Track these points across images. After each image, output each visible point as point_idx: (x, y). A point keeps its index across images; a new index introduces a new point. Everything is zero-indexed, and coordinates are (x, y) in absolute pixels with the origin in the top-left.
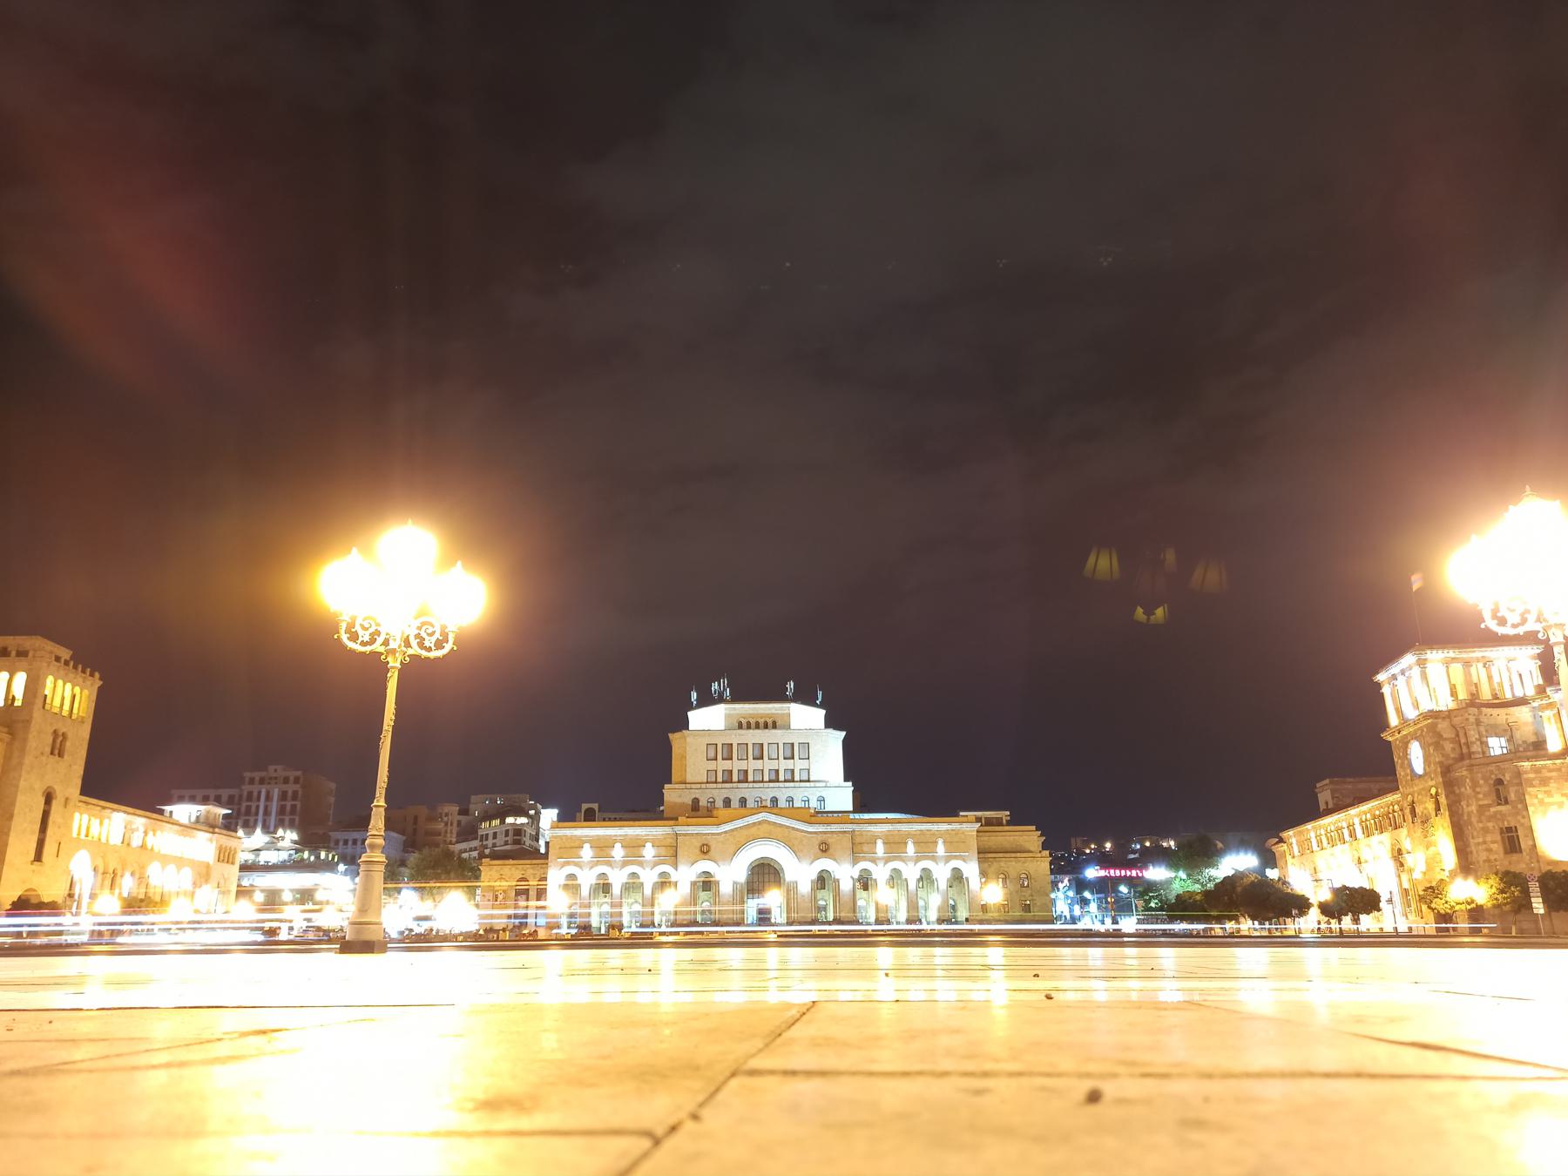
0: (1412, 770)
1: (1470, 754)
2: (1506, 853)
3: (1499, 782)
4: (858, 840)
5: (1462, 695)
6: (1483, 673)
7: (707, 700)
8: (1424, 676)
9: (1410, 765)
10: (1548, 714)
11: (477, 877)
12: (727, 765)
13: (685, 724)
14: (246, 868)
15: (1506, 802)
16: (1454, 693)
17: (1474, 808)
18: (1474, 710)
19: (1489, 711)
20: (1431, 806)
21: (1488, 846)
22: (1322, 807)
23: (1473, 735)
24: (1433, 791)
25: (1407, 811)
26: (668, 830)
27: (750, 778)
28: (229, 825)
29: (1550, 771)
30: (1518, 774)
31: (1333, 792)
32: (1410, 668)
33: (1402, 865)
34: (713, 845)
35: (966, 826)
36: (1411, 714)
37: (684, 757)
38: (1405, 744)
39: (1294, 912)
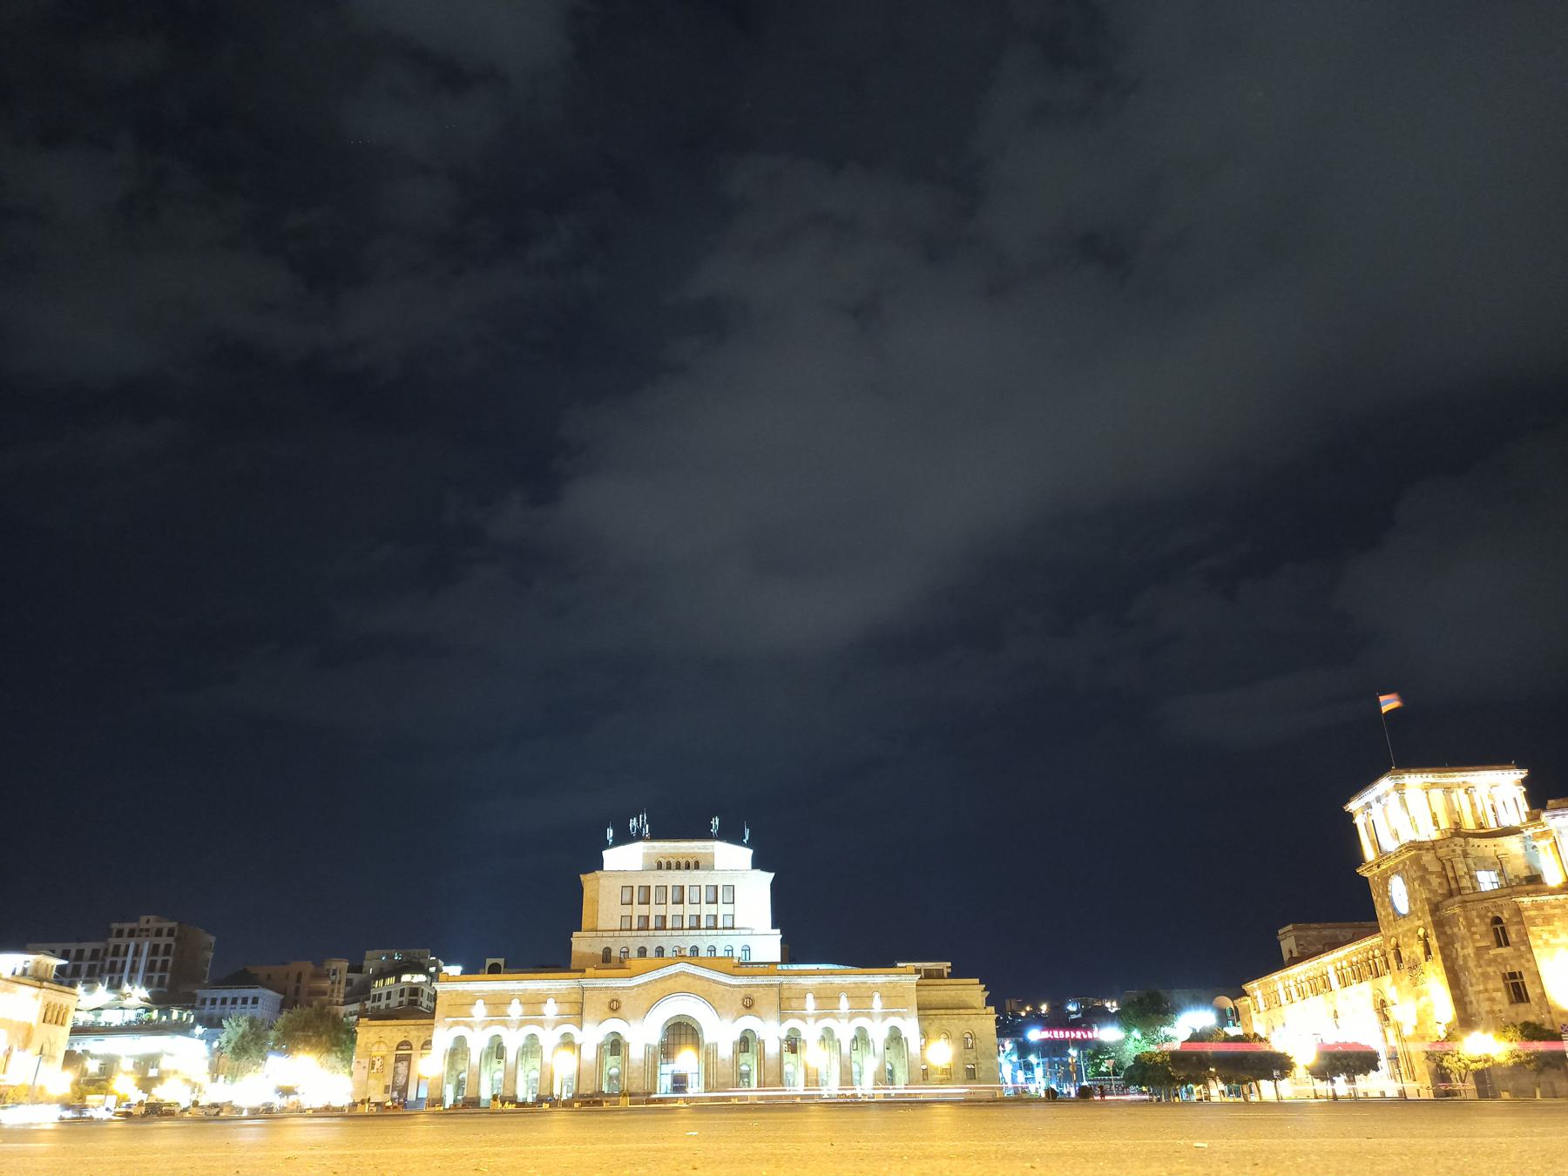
0: (1395, 909)
1: (1459, 889)
2: (1512, 1003)
3: (1497, 920)
4: (786, 994)
5: (1445, 824)
6: (1465, 800)
7: (624, 837)
8: (1404, 804)
9: (1392, 903)
10: (1543, 844)
11: (353, 1041)
12: (644, 910)
13: (598, 864)
14: (78, 1031)
15: (1507, 944)
16: (1436, 823)
17: (1470, 951)
19: (1476, 841)
20: (1419, 949)
21: (1489, 993)
22: (1286, 956)
23: (1461, 869)
24: (1421, 932)
25: (1391, 957)
26: (572, 983)
27: (669, 925)
28: (65, 978)
29: (1554, 907)
30: (1518, 911)
31: (1297, 939)
32: (1387, 795)
33: (1387, 1018)
35: (904, 978)
36: (1390, 845)
37: (596, 901)
38: (1385, 880)
39: (1276, 1073)
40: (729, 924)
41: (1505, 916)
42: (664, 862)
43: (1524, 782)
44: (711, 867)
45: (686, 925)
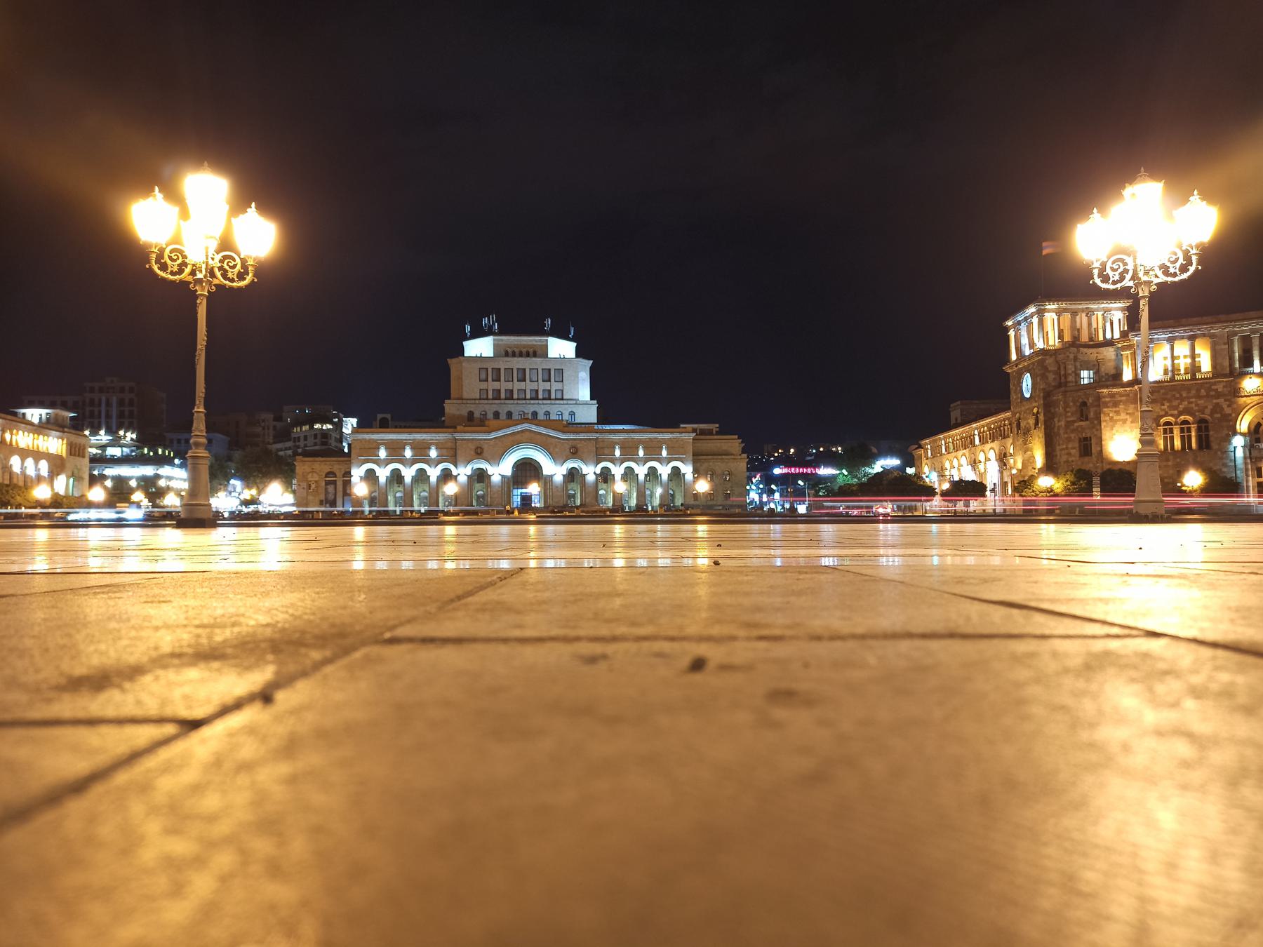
1: (1066, 382)
2: (1081, 456)
3: (1084, 404)
5: (1067, 338)
6: (1085, 319)
7: (478, 333)
12: (496, 385)
15: (1087, 419)
16: (1061, 337)
17: (1063, 423)
18: (1074, 350)
20: (1032, 422)
21: (1069, 452)
23: (1071, 368)
24: (1035, 410)
27: (515, 396)
28: (76, 426)
31: (962, 411)
32: (1032, 316)
34: (485, 447)
35: (685, 435)
37: (460, 378)
44: (545, 355)
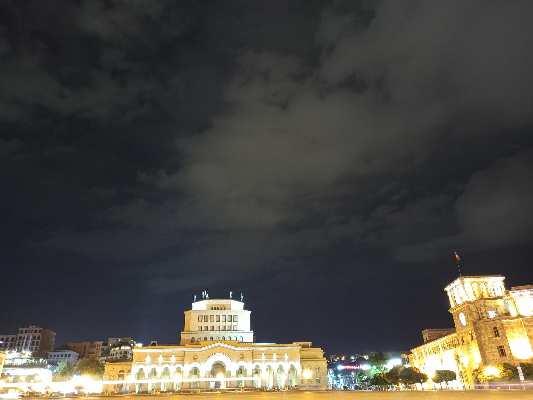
0: (461, 324)
1: (483, 317)
2: (500, 356)
3: (495, 328)
4: (255, 353)
6: (484, 287)
7: (200, 299)
8: (464, 288)
9: (460, 322)
10: (510, 302)
11: (104, 370)
13: (191, 308)
14: (6, 367)
15: (499, 336)
16: (475, 295)
17: (486, 338)
18: (482, 301)
19: (490, 301)
20: (469, 338)
22: (425, 340)
23: (483, 310)
24: (470, 332)
25: (460, 340)
27: (215, 329)
30: (502, 325)
33: (459, 362)
34: (199, 356)
35: (295, 348)
36: (459, 302)
37: (189, 321)
38: (458, 314)
39: (422, 380)
40: (235, 329)
41: (498, 326)
42: (213, 307)
43: (504, 281)
44: (230, 309)
45: (221, 329)
